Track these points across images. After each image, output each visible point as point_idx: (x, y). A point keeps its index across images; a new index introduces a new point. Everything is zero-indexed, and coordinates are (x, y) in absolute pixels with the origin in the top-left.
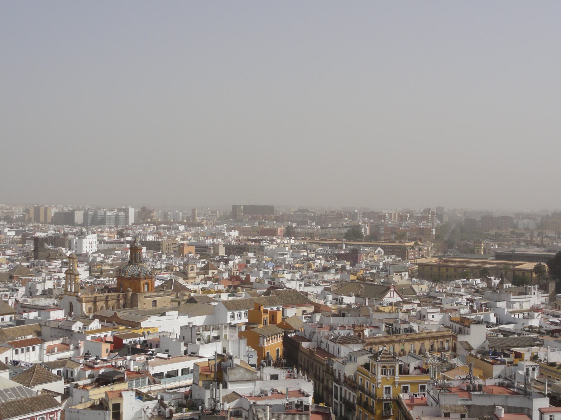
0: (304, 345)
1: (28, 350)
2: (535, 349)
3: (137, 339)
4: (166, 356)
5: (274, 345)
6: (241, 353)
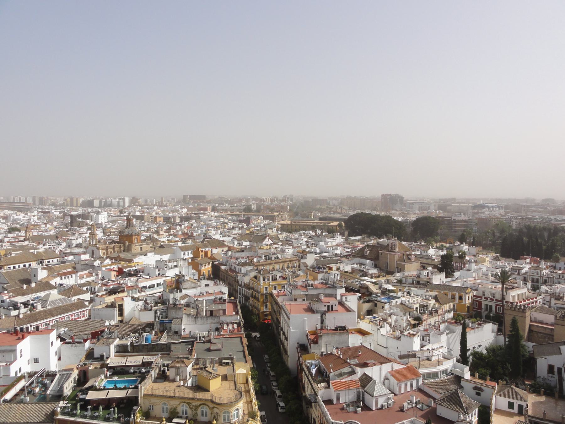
0: (223, 268)
1: (68, 277)
2: (338, 265)
3: (132, 269)
4: (148, 277)
5: (207, 269)
6: (189, 273)
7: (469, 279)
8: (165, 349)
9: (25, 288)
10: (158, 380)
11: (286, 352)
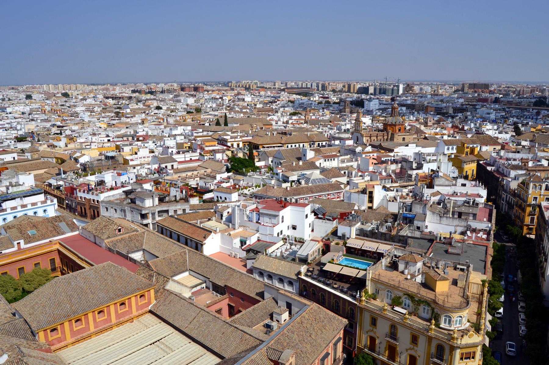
0: (489, 168)
1: (328, 160)
3: (390, 158)
5: (471, 168)
6: (448, 169)
8: (403, 241)
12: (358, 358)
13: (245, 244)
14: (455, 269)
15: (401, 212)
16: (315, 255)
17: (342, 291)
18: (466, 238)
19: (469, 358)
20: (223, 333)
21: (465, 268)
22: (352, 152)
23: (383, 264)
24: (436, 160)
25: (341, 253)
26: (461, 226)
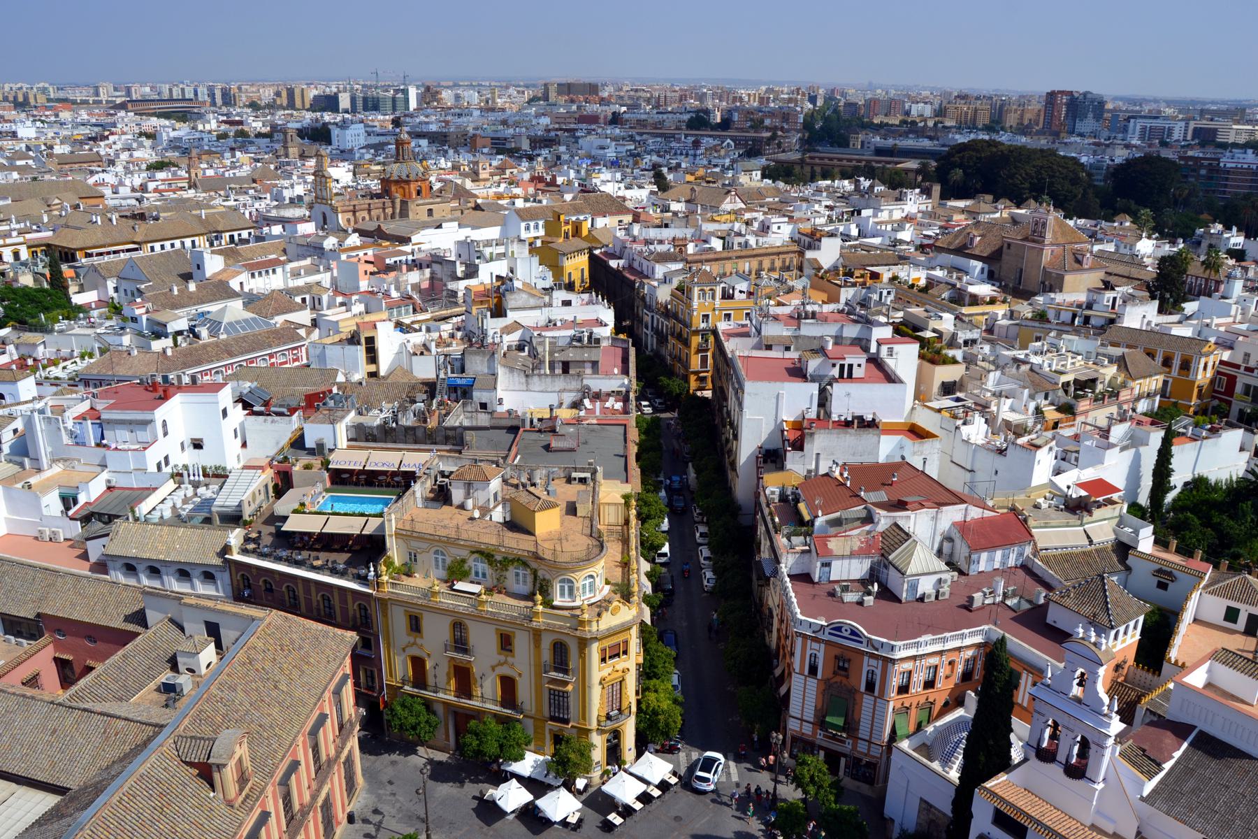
0: (613, 264)
1: (260, 273)
3: (403, 258)
5: (577, 266)
6: (530, 272)
7: (1216, 321)
8: (455, 439)
9: (176, 293)
10: (430, 504)
11: (733, 465)
12: (392, 710)
13: (75, 502)
14: (569, 480)
15: (442, 376)
16: (257, 502)
17: (334, 572)
18: (582, 413)
19: (618, 655)
20: (55, 731)
21: (588, 475)
22: (315, 249)
23: (418, 495)
24: (504, 255)
25: (319, 487)
26: (570, 391)
